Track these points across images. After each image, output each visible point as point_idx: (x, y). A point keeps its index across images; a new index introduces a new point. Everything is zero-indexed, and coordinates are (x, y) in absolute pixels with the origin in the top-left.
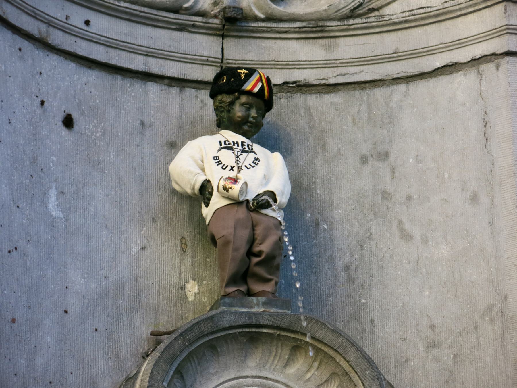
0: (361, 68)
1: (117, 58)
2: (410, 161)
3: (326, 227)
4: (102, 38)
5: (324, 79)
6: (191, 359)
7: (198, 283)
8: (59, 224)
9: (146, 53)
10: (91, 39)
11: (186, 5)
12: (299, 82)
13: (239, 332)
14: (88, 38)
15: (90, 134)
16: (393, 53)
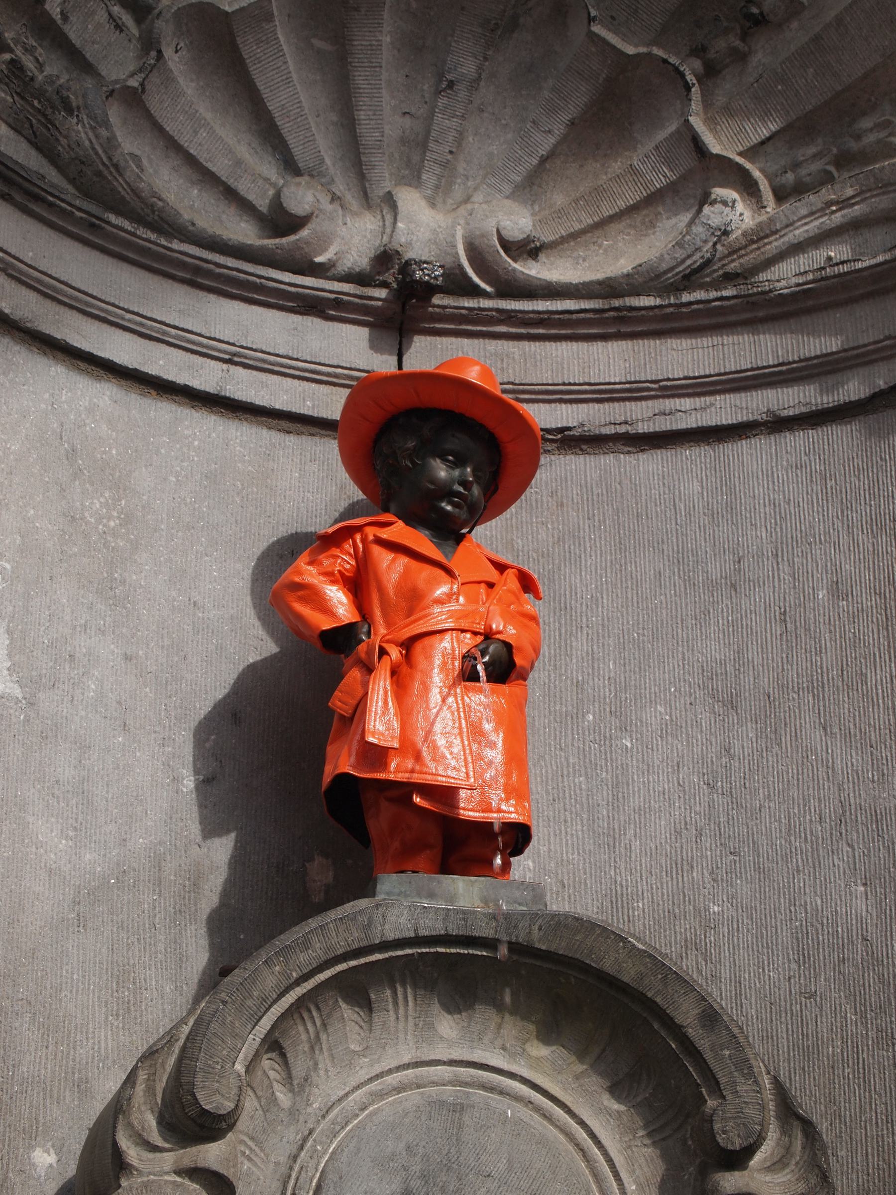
0: (709, 399)
1: (161, 362)
3: (629, 745)
4: (128, 316)
5: (626, 423)
6: (305, 1015)
8: (12, 711)
9: (227, 357)
10: (102, 314)
11: (319, 259)
12: (569, 429)
14: (97, 312)
15: (93, 520)
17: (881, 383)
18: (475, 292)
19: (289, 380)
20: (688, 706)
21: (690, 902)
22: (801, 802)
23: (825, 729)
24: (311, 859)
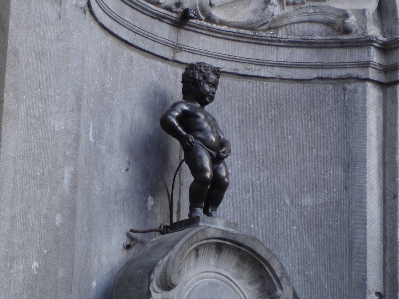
2: (290, 137)
5: (236, 70)
7: (154, 199)
13: (214, 242)
16: (285, 62)
17: (315, 76)
18: (201, 19)
19: (149, 40)
20: (248, 163)
21: (245, 223)
22: (279, 199)
23: (288, 178)
24: (148, 197)
